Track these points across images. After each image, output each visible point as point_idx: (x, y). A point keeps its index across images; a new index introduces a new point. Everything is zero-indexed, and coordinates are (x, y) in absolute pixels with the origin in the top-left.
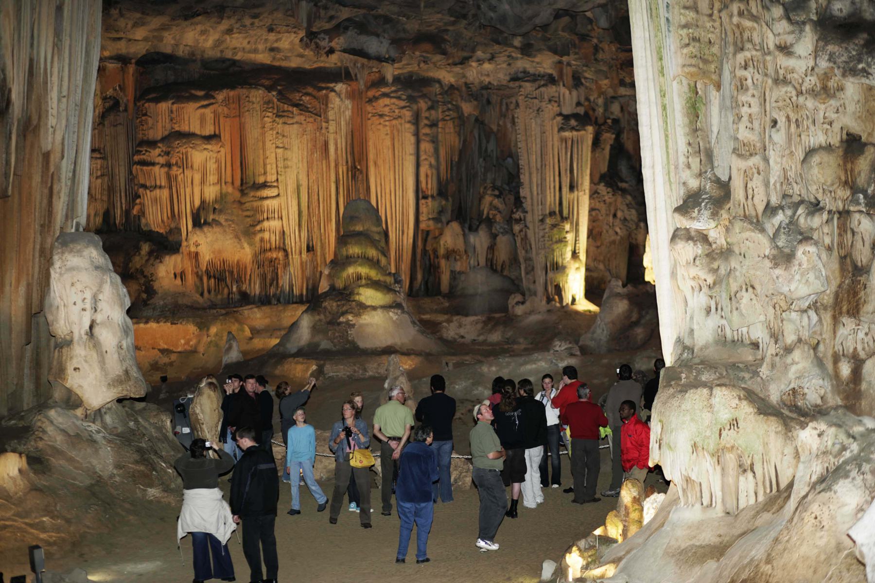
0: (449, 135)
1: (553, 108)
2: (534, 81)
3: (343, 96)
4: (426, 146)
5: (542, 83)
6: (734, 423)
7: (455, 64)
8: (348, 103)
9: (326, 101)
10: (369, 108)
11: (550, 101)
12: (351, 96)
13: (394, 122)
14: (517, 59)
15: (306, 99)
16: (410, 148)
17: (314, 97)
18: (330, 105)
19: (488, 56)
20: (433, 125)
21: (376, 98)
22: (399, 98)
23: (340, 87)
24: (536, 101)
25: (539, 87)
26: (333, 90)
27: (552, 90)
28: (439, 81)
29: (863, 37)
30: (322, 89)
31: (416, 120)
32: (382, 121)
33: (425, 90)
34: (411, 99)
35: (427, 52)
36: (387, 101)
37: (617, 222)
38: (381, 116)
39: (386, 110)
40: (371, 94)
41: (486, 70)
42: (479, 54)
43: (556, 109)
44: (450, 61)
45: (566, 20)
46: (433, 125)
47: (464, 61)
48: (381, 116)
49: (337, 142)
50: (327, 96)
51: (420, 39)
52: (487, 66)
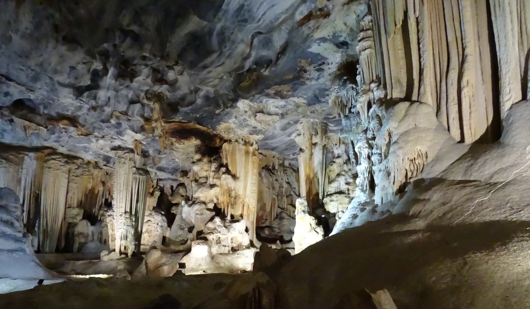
2: (123, 150)
3: (32, 158)
5: (126, 151)
7: (82, 135)
8: (35, 162)
9: (23, 159)
10: (45, 165)
11: (130, 160)
12: (37, 159)
13: (56, 171)
14: (115, 139)
15: (11, 157)
17: (16, 157)
18: (25, 162)
19: (101, 136)
21: (48, 160)
22: (60, 161)
23: (32, 154)
24: (123, 160)
25: (125, 153)
26: (27, 155)
27: (131, 155)
28: (83, 159)
30: (21, 154)
32: (50, 170)
33: (75, 161)
35: (66, 125)
36: (53, 161)
37: (158, 227)
38: (49, 168)
39: (52, 166)
40: (46, 158)
42: (96, 134)
43: (133, 164)
44: (80, 133)
45: (138, 106)
48: (49, 168)
50: (23, 158)
52: (101, 142)
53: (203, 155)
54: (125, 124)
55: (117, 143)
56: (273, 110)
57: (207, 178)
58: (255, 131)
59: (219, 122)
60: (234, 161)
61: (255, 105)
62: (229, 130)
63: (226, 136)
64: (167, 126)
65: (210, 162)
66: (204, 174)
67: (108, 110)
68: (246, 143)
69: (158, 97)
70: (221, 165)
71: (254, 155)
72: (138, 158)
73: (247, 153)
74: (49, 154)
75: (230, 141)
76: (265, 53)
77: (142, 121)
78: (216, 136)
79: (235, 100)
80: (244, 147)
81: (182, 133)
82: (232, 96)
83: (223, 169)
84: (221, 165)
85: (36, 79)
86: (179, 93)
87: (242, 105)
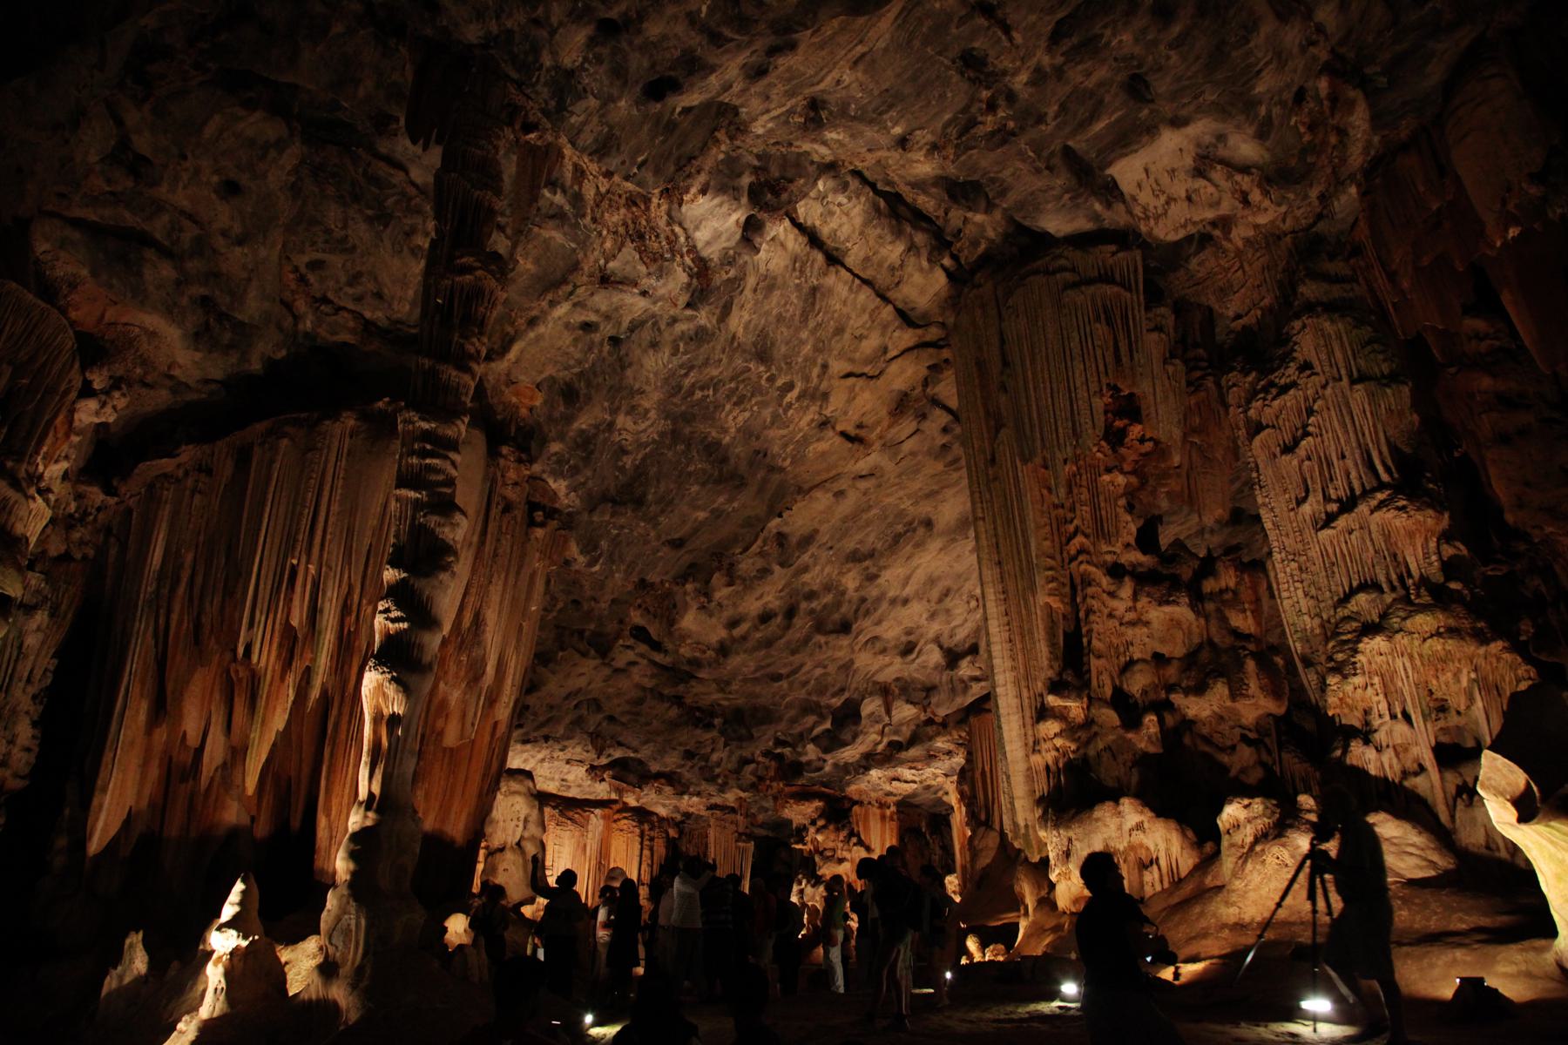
0: (660, 849)
1: (733, 827)
4: (646, 852)
6: (1139, 827)
12: (604, 817)
16: (637, 852)
20: (652, 839)
23: (598, 811)
27: (731, 817)
29: (1167, 584)
31: (642, 835)
34: (641, 823)
41: (692, 803)
45: (753, 766)
46: (652, 839)
47: (682, 794)
49: (592, 844)
51: (658, 776)
52: (695, 799)
53: (829, 821)
54: (732, 782)
55: (716, 800)
56: (910, 777)
57: (834, 850)
58: (889, 794)
59: (849, 784)
60: (867, 828)
61: (890, 773)
62: (860, 792)
63: (856, 798)
64: (787, 789)
65: (838, 830)
66: (831, 845)
67: (717, 771)
68: (882, 806)
69: (780, 757)
70: (852, 834)
71: (892, 819)
72: (740, 818)
73: (883, 817)
74: (618, 811)
75: (860, 803)
76: (896, 738)
77: (754, 779)
78: (845, 797)
79: (867, 769)
80: (878, 811)
81: (804, 796)
82: (864, 763)
83: (854, 840)
84: (852, 834)
85: (646, 742)
86: (804, 759)
87: (875, 773)
